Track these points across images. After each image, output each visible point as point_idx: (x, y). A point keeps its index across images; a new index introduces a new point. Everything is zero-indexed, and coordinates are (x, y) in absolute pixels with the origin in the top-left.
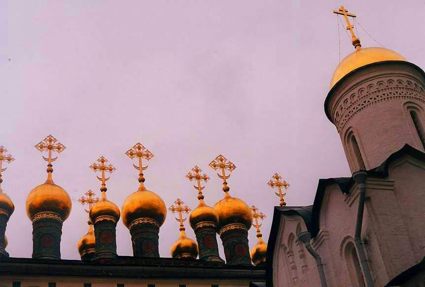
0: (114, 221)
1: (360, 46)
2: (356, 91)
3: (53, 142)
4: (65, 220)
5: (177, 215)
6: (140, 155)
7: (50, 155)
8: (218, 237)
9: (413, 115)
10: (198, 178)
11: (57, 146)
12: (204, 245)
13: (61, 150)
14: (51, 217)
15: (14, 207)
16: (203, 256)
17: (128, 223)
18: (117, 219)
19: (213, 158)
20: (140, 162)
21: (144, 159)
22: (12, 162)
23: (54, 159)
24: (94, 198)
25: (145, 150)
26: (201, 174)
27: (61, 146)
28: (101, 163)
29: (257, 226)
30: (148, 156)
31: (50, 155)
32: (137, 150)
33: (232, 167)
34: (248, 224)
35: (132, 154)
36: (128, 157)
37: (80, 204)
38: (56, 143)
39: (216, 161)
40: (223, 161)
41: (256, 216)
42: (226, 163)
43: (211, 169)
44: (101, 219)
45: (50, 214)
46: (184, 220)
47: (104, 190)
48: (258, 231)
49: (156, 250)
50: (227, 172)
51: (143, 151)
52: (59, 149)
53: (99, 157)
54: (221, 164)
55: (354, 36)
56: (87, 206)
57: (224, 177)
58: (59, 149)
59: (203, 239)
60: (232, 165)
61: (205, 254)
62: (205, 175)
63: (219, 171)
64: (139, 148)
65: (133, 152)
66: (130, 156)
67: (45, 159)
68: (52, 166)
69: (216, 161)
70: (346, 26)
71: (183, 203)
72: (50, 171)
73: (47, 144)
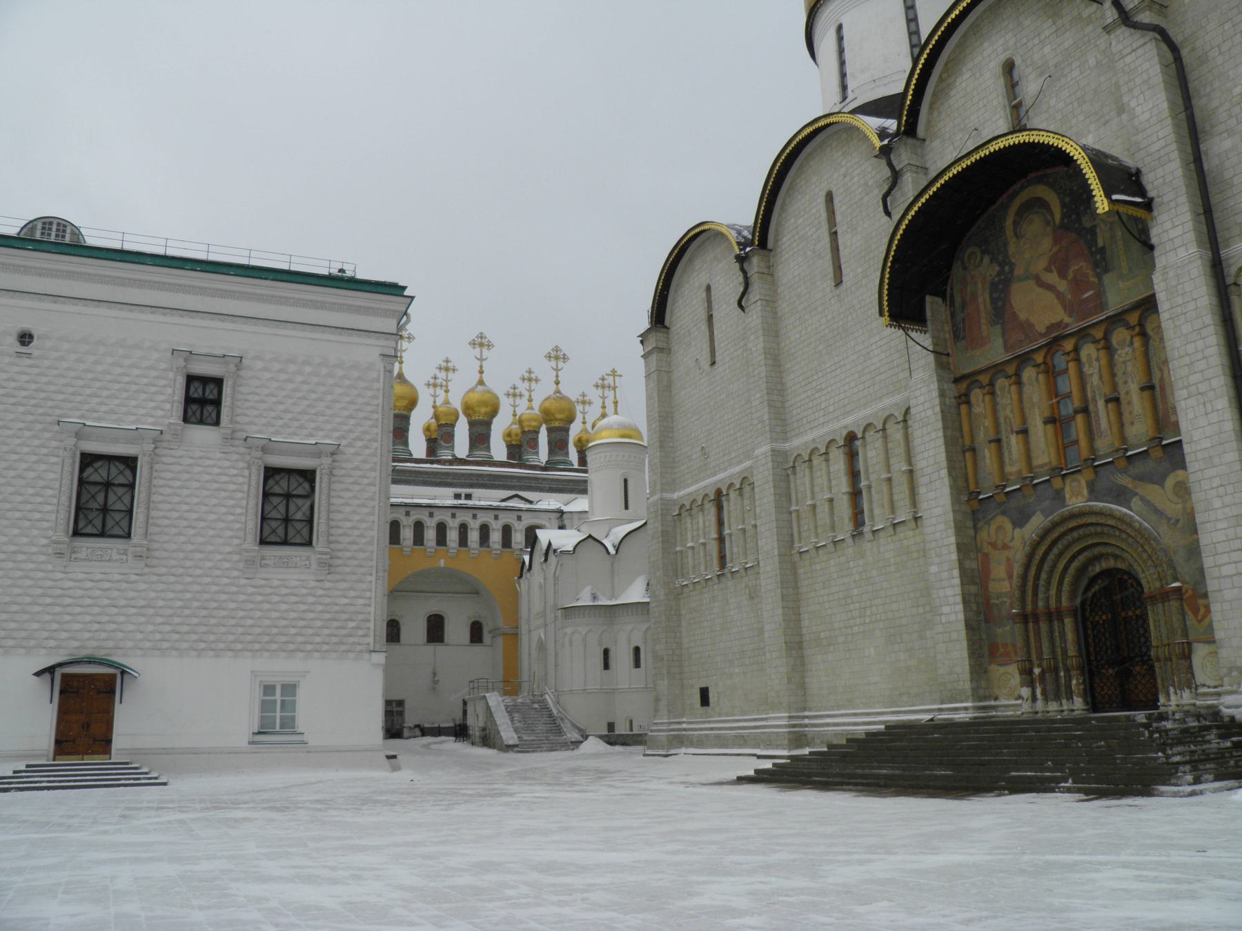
2: (598, 456)
5: (511, 400)
6: (481, 345)
9: (626, 481)
17: (467, 415)
18: (457, 418)
19: (549, 350)
21: (485, 350)
23: (405, 350)
26: (533, 376)
28: (445, 364)
29: (584, 413)
30: (488, 346)
34: (571, 420)
35: (474, 344)
37: (426, 388)
38: (407, 332)
42: (560, 354)
44: (444, 422)
48: (584, 418)
50: (561, 364)
53: (444, 358)
54: (557, 356)
55: (615, 397)
57: (557, 370)
62: (537, 377)
63: (553, 363)
64: (482, 338)
71: (517, 388)
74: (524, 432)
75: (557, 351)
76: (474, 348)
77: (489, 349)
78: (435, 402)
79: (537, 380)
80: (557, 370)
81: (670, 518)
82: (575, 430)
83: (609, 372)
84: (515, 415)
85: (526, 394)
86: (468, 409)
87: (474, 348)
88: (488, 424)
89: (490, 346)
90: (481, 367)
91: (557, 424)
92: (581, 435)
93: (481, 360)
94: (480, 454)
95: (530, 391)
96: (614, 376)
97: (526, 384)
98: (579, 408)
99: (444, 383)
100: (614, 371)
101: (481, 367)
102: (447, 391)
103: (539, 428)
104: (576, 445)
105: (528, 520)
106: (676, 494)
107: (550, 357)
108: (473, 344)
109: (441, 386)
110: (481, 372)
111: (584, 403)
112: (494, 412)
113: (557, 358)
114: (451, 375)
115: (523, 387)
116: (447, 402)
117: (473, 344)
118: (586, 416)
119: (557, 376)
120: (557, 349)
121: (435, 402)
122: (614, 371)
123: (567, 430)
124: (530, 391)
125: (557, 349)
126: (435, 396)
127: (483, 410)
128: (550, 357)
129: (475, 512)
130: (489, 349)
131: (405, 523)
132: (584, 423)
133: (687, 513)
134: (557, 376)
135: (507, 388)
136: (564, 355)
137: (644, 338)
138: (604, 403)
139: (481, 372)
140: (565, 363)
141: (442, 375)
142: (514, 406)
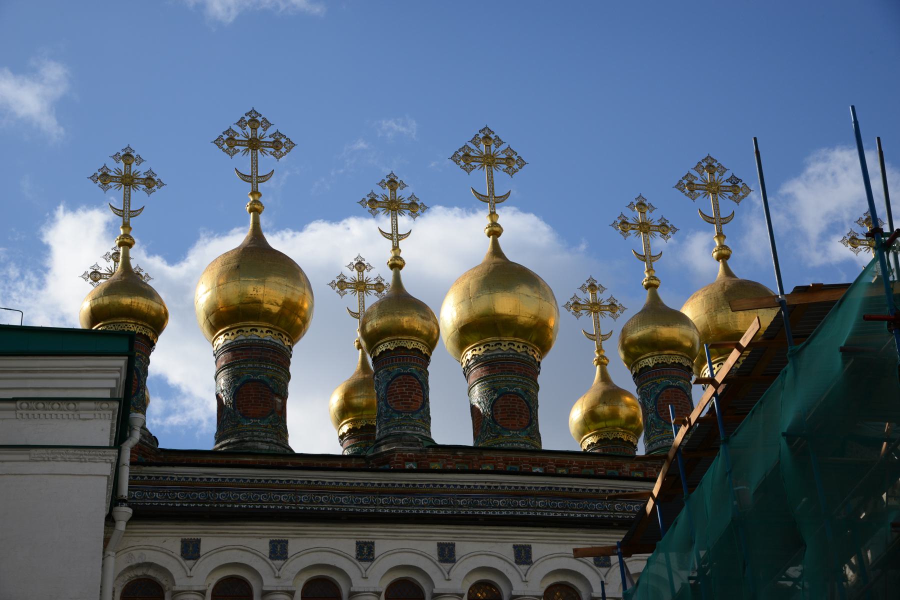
0: (424, 350)
3: (260, 130)
4: (297, 341)
5: (588, 321)
6: (490, 161)
7: (255, 164)
11: (272, 140)
12: (658, 417)
13: (283, 150)
14: (262, 336)
15: (166, 314)
16: (655, 446)
19: (688, 166)
21: (499, 174)
22: (158, 192)
23: (265, 178)
24: (370, 276)
25: (503, 147)
27: (283, 140)
28: (388, 192)
31: (255, 164)
32: (483, 147)
37: (334, 293)
38: (271, 131)
40: (717, 174)
43: (682, 198)
44: (391, 347)
45: (259, 330)
46: (605, 337)
47: (396, 265)
49: (530, 424)
52: (276, 144)
56: (352, 299)
58: (276, 144)
59: (655, 404)
60: (740, 184)
61: (662, 439)
65: (472, 154)
67: (244, 177)
68: (260, 195)
72: (256, 211)
73: (247, 137)
75: (711, 168)
76: (468, 169)
77: (511, 172)
87: (468, 169)
130: (511, 172)
131: (269, 583)
140: (738, 202)
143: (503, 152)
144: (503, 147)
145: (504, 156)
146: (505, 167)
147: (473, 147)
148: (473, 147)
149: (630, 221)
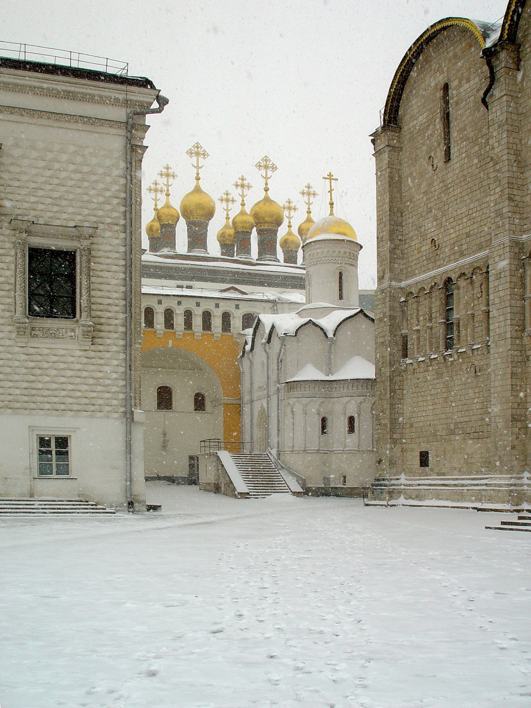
1: (333, 207)
5: (224, 204)
6: (198, 154)
8: (255, 229)
10: (243, 186)
17: (184, 216)
19: (259, 159)
20: (198, 162)
21: (201, 159)
25: (203, 149)
29: (289, 218)
30: (204, 155)
32: (196, 149)
33: (274, 168)
35: (191, 153)
36: (187, 157)
39: (261, 161)
41: (289, 208)
42: (270, 164)
50: (270, 173)
51: (201, 151)
55: (331, 199)
57: (266, 178)
60: (275, 166)
62: (248, 184)
63: (263, 172)
65: (192, 151)
66: (189, 155)
69: (261, 161)
70: (329, 190)
74: (237, 232)
75: (266, 161)
77: (204, 158)
78: (156, 205)
79: (249, 187)
80: (266, 178)
81: (397, 305)
82: (282, 232)
83: (327, 177)
84: (228, 218)
85: (239, 200)
86: (186, 213)
88: (204, 226)
89: (205, 155)
90: (198, 174)
91: (266, 227)
92: (287, 237)
93: (198, 167)
94: (196, 253)
95: (243, 196)
96: (331, 179)
97: (239, 190)
98: (286, 213)
99: (165, 188)
100: (330, 175)
101: (198, 174)
102: (168, 195)
103: (251, 230)
104: (282, 246)
105: (245, 309)
106: (403, 283)
107: (260, 166)
108: (190, 153)
109: (161, 191)
110: (198, 179)
111: (289, 208)
112: (210, 214)
113: (266, 167)
114: (171, 181)
115: (235, 193)
116: (168, 206)
117: (190, 153)
118: (292, 220)
119: (266, 184)
120: (266, 159)
121: (156, 205)
122: (330, 175)
123: (275, 232)
124: (243, 196)
125: (266, 159)
126: (156, 200)
127: (200, 212)
128: (260, 166)
129: (198, 300)
130: (204, 158)
132: (290, 226)
133: (413, 300)
134: (266, 184)
135: (221, 194)
136: (273, 164)
137: (375, 138)
138: (309, 209)
139: (198, 179)
141: (164, 180)
142: (227, 210)
143: (202, 151)
144: (203, 149)
145: (202, 153)
146: (202, 156)
147: (193, 149)
148: (193, 149)
149: (238, 184)
